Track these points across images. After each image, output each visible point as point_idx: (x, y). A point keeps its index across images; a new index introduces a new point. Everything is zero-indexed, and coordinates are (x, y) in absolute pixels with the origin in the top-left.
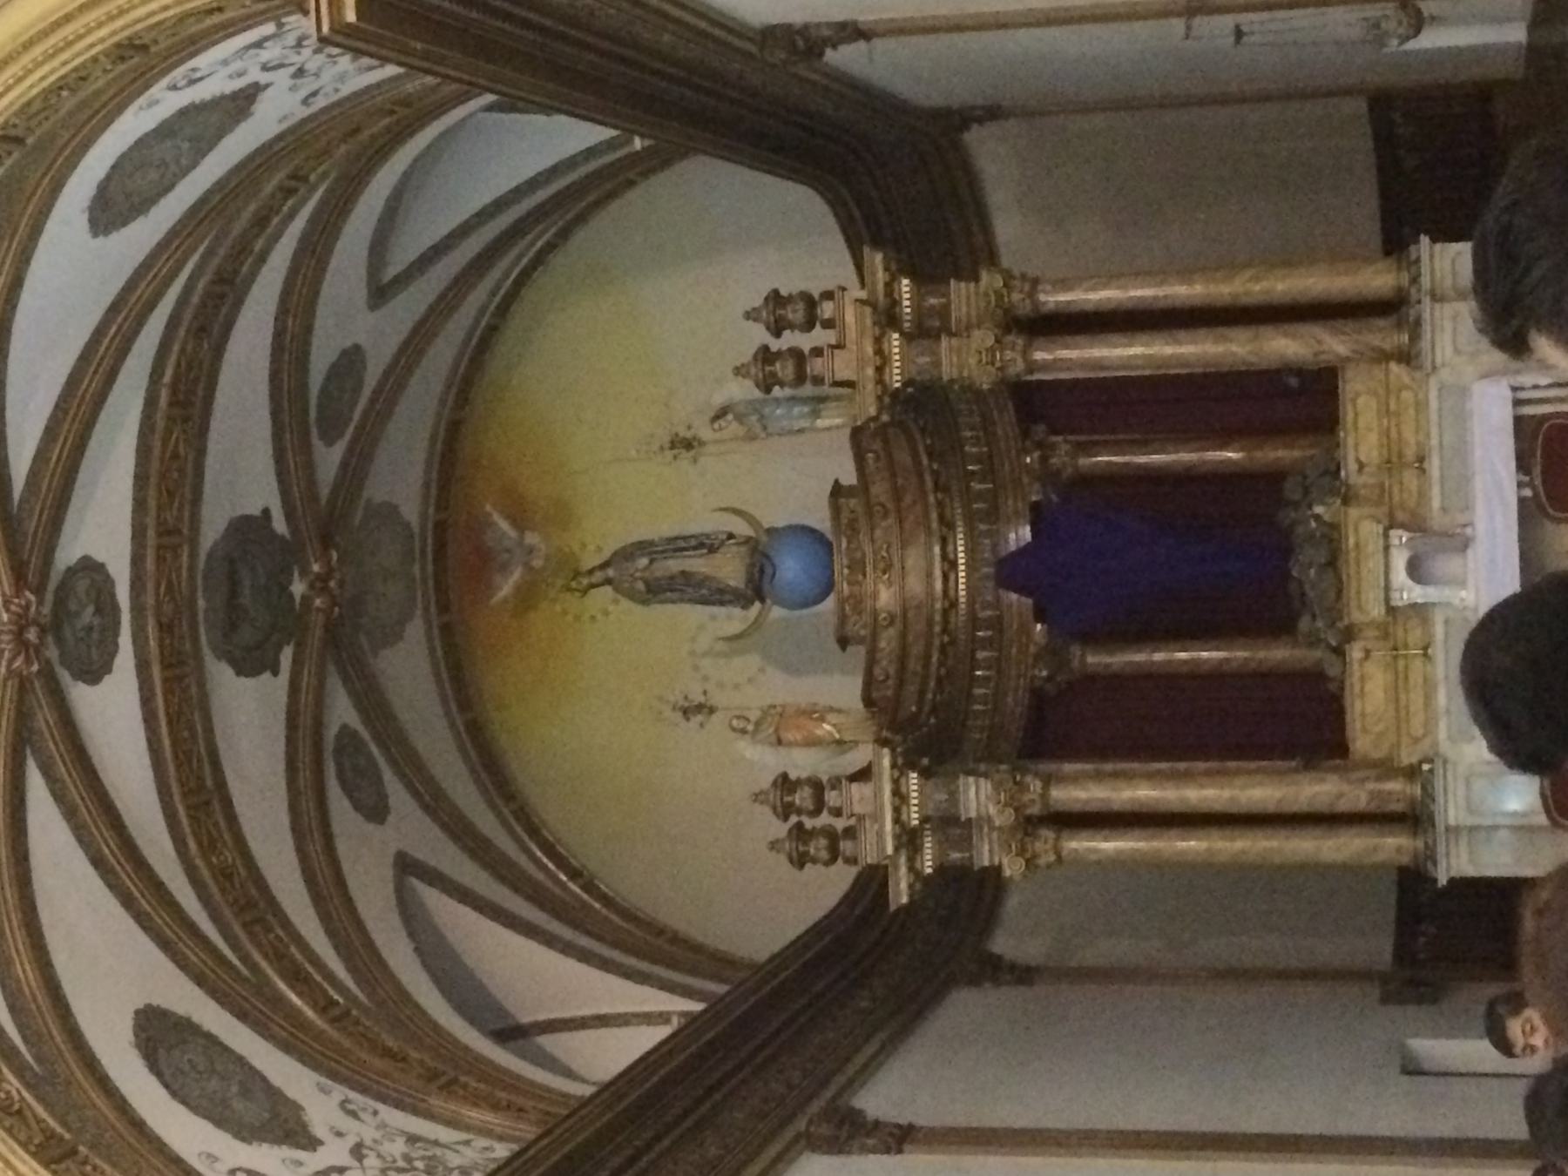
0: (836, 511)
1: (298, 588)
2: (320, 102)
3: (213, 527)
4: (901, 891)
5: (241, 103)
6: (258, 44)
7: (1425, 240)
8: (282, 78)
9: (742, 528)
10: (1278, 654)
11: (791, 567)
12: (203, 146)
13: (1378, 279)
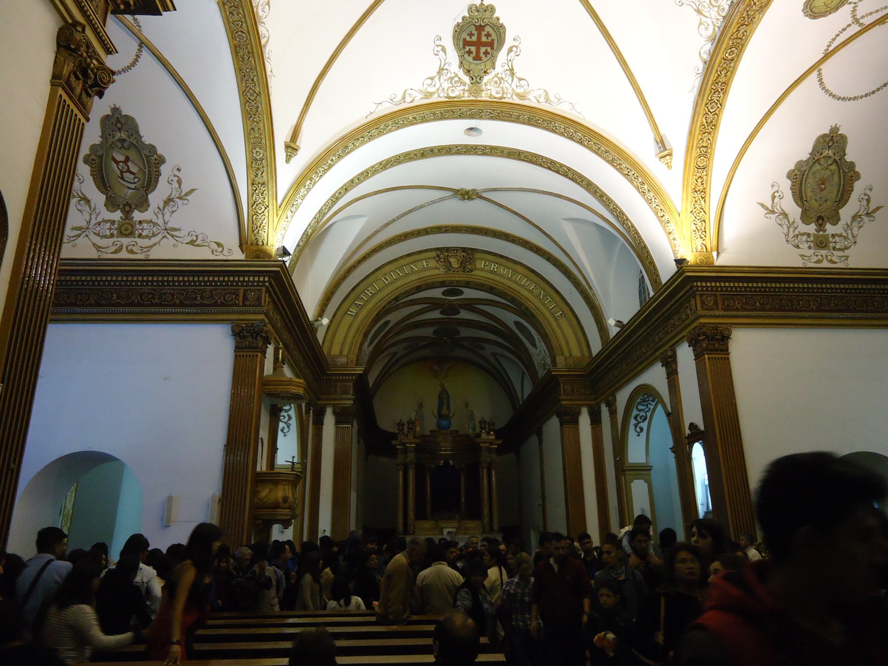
0: (454, 431)
1: (445, 338)
2: (532, 355)
3: (459, 328)
4: (394, 442)
5: (534, 345)
6: (545, 352)
7: (502, 535)
8: (538, 352)
9: (451, 415)
10: (429, 509)
11: (444, 423)
12: (527, 339)
13: (496, 527)
